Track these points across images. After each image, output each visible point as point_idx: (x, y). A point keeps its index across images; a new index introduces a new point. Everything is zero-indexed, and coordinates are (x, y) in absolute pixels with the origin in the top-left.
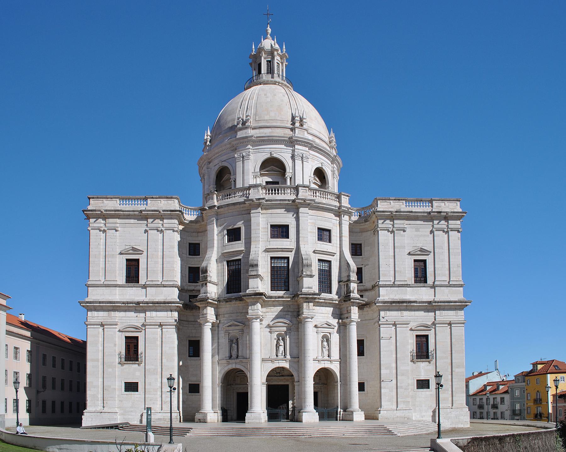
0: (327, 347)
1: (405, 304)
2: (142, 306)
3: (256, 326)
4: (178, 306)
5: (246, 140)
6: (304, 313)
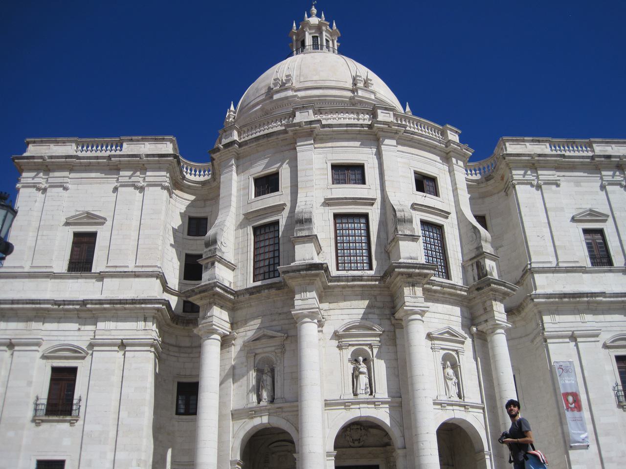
0: (454, 379)
1: (586, 299)
2: (90, 310)
3: (309, 330)
4: (158, 310)
5: (286, 102)
6: (407, 304)
